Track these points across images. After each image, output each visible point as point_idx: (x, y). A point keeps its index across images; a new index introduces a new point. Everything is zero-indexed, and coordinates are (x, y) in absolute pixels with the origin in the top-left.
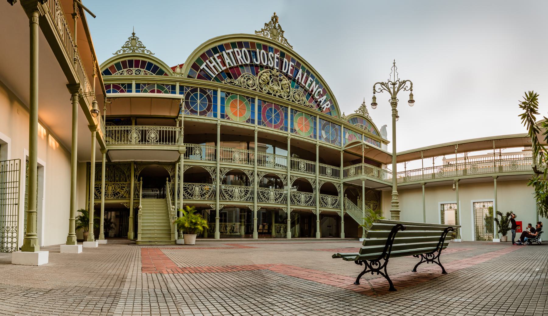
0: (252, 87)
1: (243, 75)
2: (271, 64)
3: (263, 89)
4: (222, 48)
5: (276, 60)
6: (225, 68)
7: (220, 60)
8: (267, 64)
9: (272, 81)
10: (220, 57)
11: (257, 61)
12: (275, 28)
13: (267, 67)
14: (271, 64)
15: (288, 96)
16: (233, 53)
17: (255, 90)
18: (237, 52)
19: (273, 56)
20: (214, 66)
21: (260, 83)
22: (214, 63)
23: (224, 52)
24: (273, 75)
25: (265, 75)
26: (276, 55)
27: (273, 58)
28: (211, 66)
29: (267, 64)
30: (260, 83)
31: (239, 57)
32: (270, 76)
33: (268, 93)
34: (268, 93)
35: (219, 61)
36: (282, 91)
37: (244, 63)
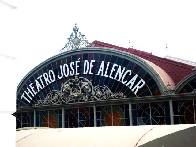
0: (56, 102)
1: (49, 94)
2: (72, 73)
3: (66, 100)
4: (36, 76)
5: (77, 66)
6: (37, 92)
7: (33, 87)
8: (69, 74)
9: (73, 90)
10: (34, 85)
11: (60, 76)
12: (76, 37)
13: (70, 77)
14: (72, 73)
15: (89, 97)
16: (43, 78)
17: (59, 103)
18: (46, 75)
19: (74, 64)
20: (30, 94)
21: (63, 96)
22: (30, 91)
23: (36, 80)
24: (74, 83)
25: (66, 86)
26: (77, 62)
27: (74, 67)
28: (27, 94)
29: (69, 74)
30: (63, 96)
31: (46, 80)
32: (71, 86)
33: (70, 102)
34: (70, 102)
35: (32, 88)
36: (82, 94)
37: (50, 83)
